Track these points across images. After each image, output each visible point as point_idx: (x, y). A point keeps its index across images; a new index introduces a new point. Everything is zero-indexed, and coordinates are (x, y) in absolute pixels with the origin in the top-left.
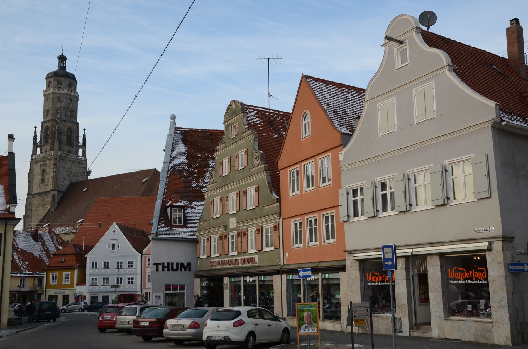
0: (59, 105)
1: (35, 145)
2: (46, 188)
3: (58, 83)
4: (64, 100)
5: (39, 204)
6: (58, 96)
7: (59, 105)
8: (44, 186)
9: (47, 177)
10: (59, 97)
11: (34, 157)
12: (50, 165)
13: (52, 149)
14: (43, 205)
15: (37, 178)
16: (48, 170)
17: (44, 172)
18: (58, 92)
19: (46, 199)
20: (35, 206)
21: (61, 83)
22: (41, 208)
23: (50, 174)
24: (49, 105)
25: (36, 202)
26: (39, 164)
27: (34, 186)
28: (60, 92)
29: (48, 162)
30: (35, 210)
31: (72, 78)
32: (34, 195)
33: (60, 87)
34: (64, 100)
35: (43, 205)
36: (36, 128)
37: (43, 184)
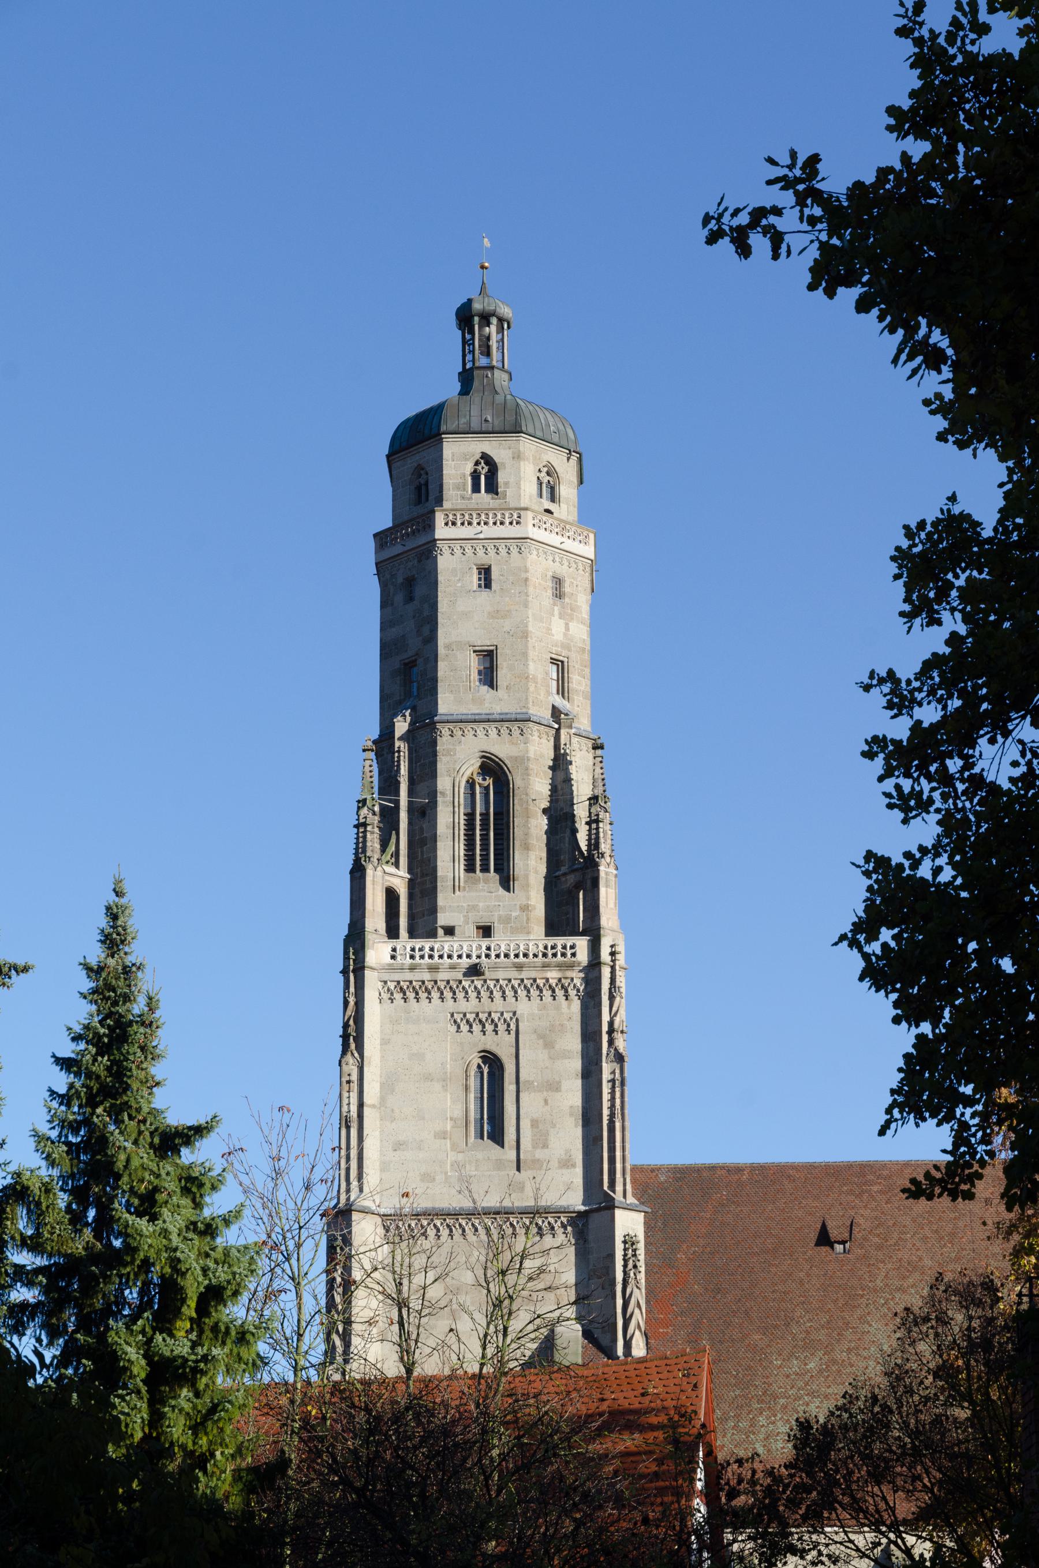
8: (499, 1165)
23: (554, 1086)
24: (496, 614)
26: (434, 1011)
29: (526, 1008)
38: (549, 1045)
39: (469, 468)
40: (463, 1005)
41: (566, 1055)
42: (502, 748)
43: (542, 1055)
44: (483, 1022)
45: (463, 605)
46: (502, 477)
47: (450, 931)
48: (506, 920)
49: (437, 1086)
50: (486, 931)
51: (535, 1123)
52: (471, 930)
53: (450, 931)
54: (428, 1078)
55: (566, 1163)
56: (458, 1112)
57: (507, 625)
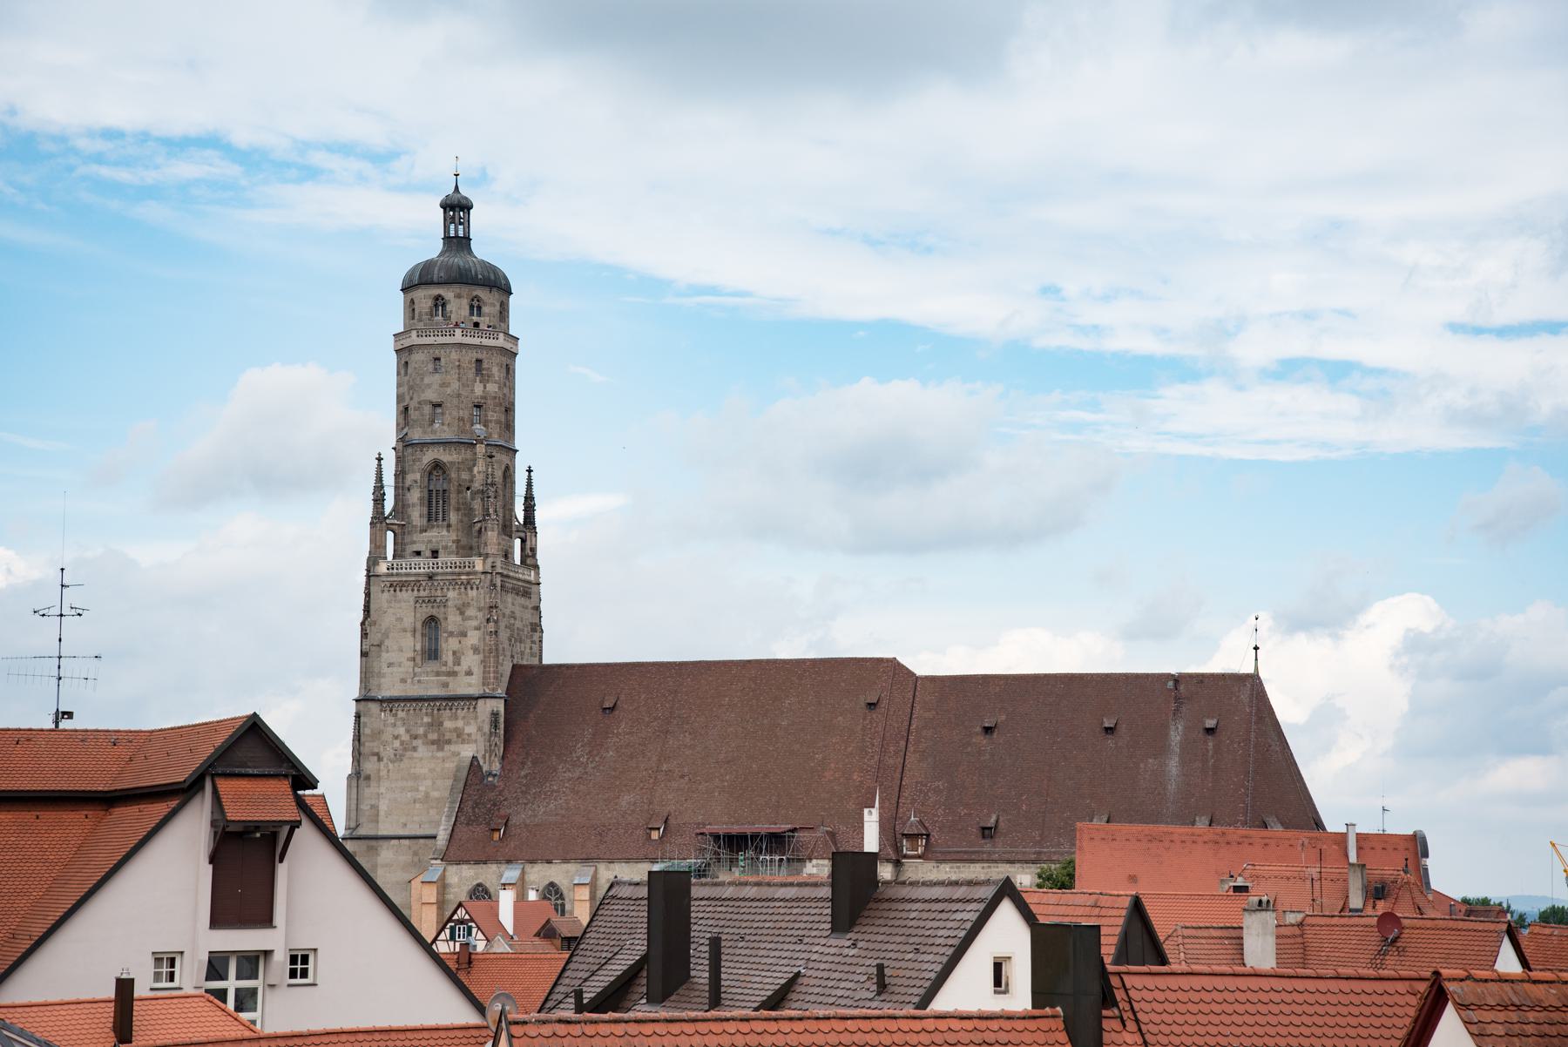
0: (478, 389)
1: (378, 520)
2: (446, 685)
3: (472, 307)
4: (495, 370)
5: (416, 737)
6: (475, 355)
7: (478, 389)
8: (438, 674)
9: (449, 646)
10: (479, 361)
11: (382, 568)
12: (466, 605)
13: (466, 549)
14: (440, 743)
15: (402, 646)
16: (452, 620)
17: (432, 622)
18: (476, 341)
19: (448, 724)
20: (397, 744)
21: (479, 308)
22: (423, 751)
23: (464, 634)
24: (444, 385)
25: (402, 731)
26: (407, 596)
27: (385, 670)
28: (486, 342)
29: (451, 594)
30: (398, 757)
31: (498, 284)
32: (390, 702)
33: (476, 325)
34: (495, 370)
35: (440, 743)
36: (380, 459)
37: (433, 666)
38: (462, 613)
39: (430, 303)
40: (422, 593)
41: (470, 618)
42: (446, 457)
43: (459, 618)
44: (431, 601)
45: (426, 381)
46: (448, 308)
47: (418, 553)
48: (445, 548)
49: (409, 634)
50: (435, 554)
51: (454, 653)
52: (428, 553)
53: (418, 553)
54: (405, 630)
55: (469, 673)
56: (418, 647)
57: (449, 391)
